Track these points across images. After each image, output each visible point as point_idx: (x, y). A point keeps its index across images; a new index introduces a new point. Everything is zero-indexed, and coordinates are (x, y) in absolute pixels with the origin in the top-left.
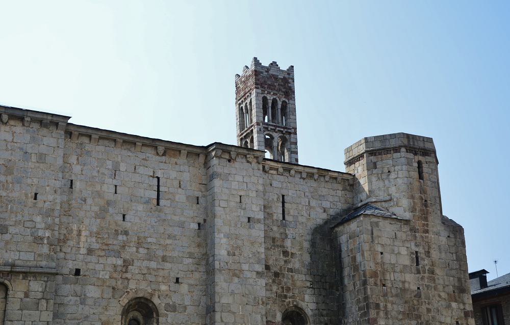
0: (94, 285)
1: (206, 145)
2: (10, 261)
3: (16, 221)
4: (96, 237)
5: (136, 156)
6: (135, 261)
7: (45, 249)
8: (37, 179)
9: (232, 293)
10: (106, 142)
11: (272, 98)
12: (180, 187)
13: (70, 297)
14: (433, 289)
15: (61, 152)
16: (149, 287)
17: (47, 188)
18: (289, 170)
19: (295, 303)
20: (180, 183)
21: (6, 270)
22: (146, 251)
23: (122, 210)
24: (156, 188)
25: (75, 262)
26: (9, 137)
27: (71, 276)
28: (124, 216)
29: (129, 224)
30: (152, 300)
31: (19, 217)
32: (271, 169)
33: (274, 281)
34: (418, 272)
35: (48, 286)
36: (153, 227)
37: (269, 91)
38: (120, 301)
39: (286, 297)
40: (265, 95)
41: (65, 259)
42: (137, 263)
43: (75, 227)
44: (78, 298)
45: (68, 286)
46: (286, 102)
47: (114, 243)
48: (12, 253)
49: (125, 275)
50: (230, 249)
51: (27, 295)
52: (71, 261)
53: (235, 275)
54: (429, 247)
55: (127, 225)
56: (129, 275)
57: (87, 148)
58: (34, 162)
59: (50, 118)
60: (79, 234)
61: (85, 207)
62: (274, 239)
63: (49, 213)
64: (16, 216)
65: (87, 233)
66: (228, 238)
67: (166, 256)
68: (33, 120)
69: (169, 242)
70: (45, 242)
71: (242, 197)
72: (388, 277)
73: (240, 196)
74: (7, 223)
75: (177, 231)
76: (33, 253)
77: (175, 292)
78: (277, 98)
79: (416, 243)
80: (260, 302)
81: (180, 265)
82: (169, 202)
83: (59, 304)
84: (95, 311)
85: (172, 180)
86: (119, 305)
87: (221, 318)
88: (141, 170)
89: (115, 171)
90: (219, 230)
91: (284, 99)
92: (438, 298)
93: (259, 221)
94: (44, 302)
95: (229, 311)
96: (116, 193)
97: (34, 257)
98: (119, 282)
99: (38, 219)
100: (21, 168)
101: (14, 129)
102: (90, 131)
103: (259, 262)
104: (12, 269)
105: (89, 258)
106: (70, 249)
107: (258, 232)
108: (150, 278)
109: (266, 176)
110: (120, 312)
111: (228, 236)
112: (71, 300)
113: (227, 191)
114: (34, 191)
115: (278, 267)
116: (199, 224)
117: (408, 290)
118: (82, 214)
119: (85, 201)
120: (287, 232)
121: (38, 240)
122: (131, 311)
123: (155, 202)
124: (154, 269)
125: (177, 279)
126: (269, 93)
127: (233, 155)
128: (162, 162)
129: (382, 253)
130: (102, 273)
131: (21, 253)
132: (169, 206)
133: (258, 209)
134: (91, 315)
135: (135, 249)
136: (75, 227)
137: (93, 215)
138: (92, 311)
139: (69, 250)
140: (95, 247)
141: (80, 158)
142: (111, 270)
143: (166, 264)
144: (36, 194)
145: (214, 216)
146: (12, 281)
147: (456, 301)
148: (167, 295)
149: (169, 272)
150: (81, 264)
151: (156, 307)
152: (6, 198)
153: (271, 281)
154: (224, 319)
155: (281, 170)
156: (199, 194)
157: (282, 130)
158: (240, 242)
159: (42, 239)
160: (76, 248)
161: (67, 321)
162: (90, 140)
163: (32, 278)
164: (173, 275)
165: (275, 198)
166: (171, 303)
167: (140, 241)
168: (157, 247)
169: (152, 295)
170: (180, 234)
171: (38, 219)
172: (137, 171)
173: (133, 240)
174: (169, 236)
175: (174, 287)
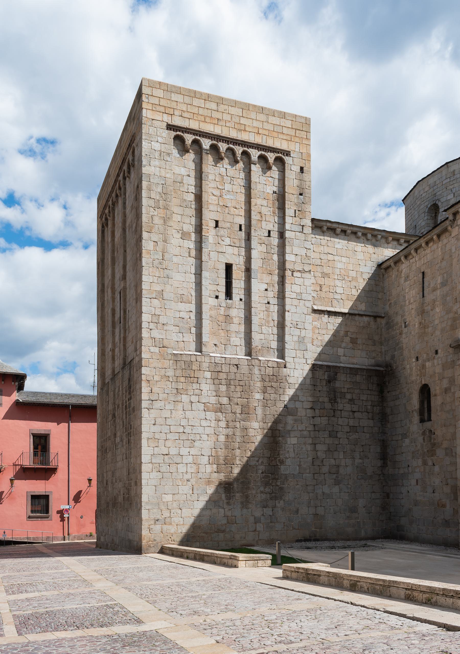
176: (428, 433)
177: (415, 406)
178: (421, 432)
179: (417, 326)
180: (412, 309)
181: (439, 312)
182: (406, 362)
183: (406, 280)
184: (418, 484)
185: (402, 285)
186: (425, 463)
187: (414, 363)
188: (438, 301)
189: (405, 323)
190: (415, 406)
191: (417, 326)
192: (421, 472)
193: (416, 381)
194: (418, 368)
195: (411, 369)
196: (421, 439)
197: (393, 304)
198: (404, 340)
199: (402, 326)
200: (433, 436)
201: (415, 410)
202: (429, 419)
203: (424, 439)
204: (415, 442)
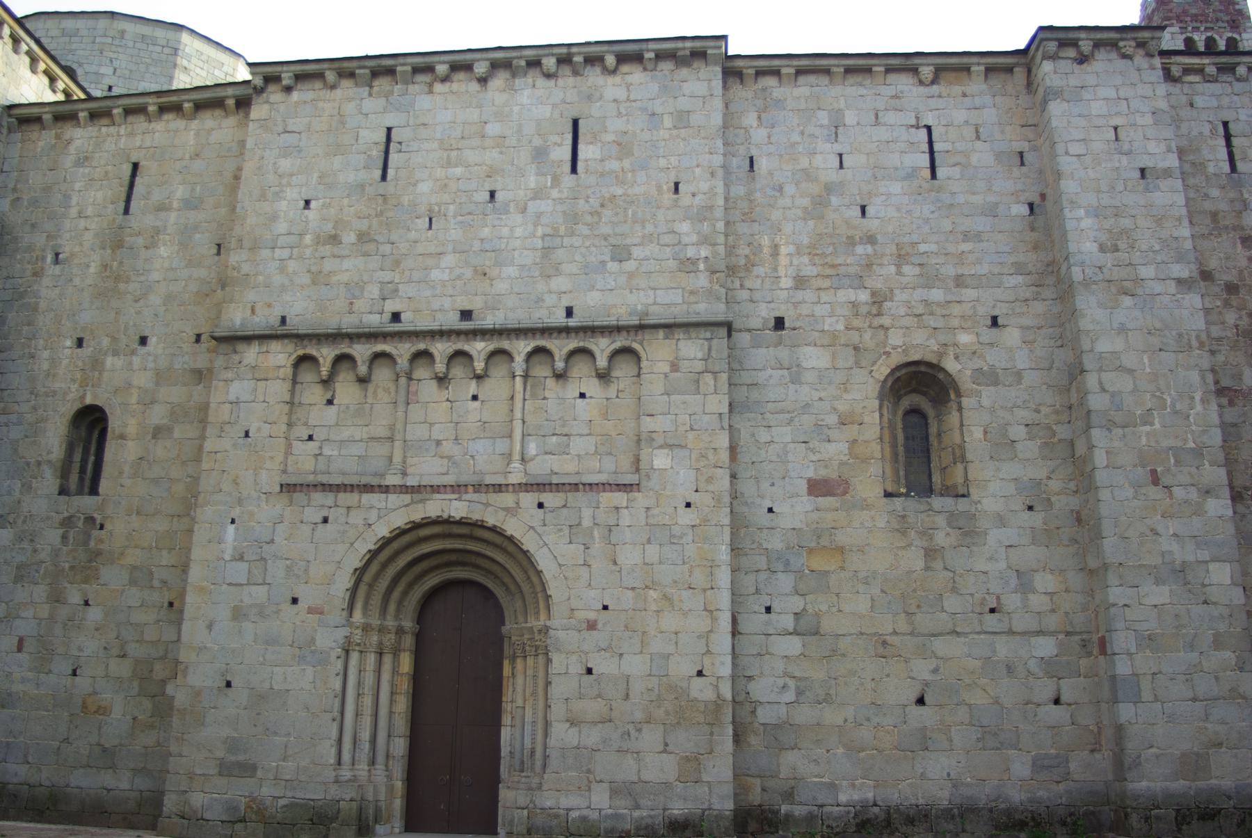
0: (815, 345)
1: (1022, 46)
2: (639, 307)
3: (643, 237)
4: (810, 254)
5: (876, 94)
6: (897, 292)
7: (702, 281)
8: (676, 157)
9: (1122, 330)
10: (812, 79)
11: (1204, 37)
12: (978, 138)
13: (769, 371)
15: (718, 103)
16: (933, 341)
17: (698, 170)
18: (1231, 69)
20: (977, 132)
21: (631, 323)
22: (917, 270)
23: (858, 198)
24: (925, 147)
25: (772, 305)
26: (621, 94)
27: (768, 332)
28: (863, 210)
29: (876, 223)
30: (942, 365)
31: (649, 228)
32: (1187, 71)
33: (1227, 304)
35: (714, 348)
36: (927, 221)
37: (1195, 25)
38: (872, 371)
41: (751, 301)
42: (900, 296)
43: (766, 241)
44: (785, 372)
45: (763, 351)
46: (1235, 39)
47: (848, 261)
48: (642, 293)
49: (877, 321)
50: (1104, 237)
51: (675, 367)
52: (766, 304)
55: (871, 224)
56: (886, 321)
57: (775, 94)
58: (670, 129)
59: (688, 44)
61: (781, 202)
62: (1214, 215)
63: (702, 215)
64: (644, 227)
65: (791, 249)
66: (1097, 216)
67: (963, 275)
68: (660, 56)
69: (966, 247)
70: (702, 266)
71: (1119, 129)
73: (1116, 129)
74: (628, 241)
75: (981, 224)
76: (680, 290)
77: (991, 344)
80: (1195, 343)
81: (999, 290)
82: (957, 169)
83: (748, 385)
84: (823, 394)
85: (959, 126)
86: (871, 380)
87: (1100, 383)
88: (890, 118)
89: (836, 127)
90: (1072, 202)
91: (1230, 35)
93: (1167, 173)
94: (708, 378)
95: (1120, 368)
96: (841, 166)
97: (683, 296)
98: (867, 336)
99: (685, 227)
100: (646, 142)
101: (629, 78)
102: (776, 62)
103: (1180, 258)
104: (643, 322)
105: (800, 295)
106: (759, 281)
107: (1170, 196)
108: (932, 322)
109: (1175, 89)
110: (876, 394)
111: (1097, 212)
112: (771, 377)
113: (1082, 122)
114: (673, 179)
116: (1031, 206)
118: (776, 215)
119: (781, 189)
120: (1246, 196)
121: (688, 266)
122: (906, 394)
123: (927, 173)
124: (938, 304)
126: (1196, 29)
127: (1086, 46)
128: (933, 97)
130: (828, 321)
131: (657, 291)
132: (958, 176)
133: (1163, 147)
134: (815, 403)
135: (893, 269)
136: (766, 241)
137: (799, 213)
138: (816, 395)
139: (757, 284)
140: (809, 273)
141: (763, 115)
142: (847, 313)
143: (964, 291)
144: (677, 185)
145: (1058, 175)
146: (645, 343)
148: (974, 353)
149: (974, 307)
150: (783, 307)
151: (953, 380)
152: (623, 198)
153: (1218, 303)
154: (1107, 387)
155: (1211, 70)
156: (1024, 146)
158: (1126, 223)
159: (693, 262)
160: (772, 280)
161: (768, 415)
162: (780, 79)
163: (681, 336)
164: (985, 311)
165: (1206, 129)
166: (985, 368)
167: (903, 252)
168: (941, 260)
169: (941, 355)
170: (988, 229)
171: (685, 227)
172: (880, 120)
173: (888, 251)
174: (965, 235)
175: (989, 334)
176: (80, 524)
177: (49, 452)
178: (58, 518)
179: (92, 270)
180: (87, 229)
181: (168, 257)
182: (41, 342)
183: (79, 163)
184: (24, 649)
185: (66, 170)
186: (57, 598)
187: (67, 350)
188: (169, 235)
189: (57, 255)
190: (49, 452)
191: (92, 270)
192: (41, 619)
193: (65, 394)
194: (80, 363)
195: (54, 361)
196: (53, 536)
197: (26, 203)
198: (46, 290)
199: (44, 258)
200: (96, 533)
201: (49, 462)
202: (94, 491)
203: (64, 537)
204: (32, 541)
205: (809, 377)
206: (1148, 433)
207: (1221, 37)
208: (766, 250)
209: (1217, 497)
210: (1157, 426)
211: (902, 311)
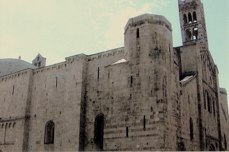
11: (188, 13)
14: (139, 93)
19: (101, 113)
32: (94, 58)
33: (93, 105)
34: (131, 86)
39: (97, 111)
40: (184, 13)
43: (35, 102)
51: (19, 125)
53: (70, 107)
54: (139, 71)
56: (47, 114)
60: (36, 104)
69: (59, 99)
72: (115, 93)
78: (190, 12)
79: (131, 71)
92: (141, 97)
115: (95, 99)
117: (124, 97)
124: (54, 110)
125: (60, 112)
126: (185, 11)
129: (113, 83)
136: (35, 102)
147: (152, 96)
157: (193, 24)
169: (53, 119)
205: (38, 125)
206: (69, 133)
207: (192, 12)
208: (35, 103)
209: (77, 144)
210: (71, 132)
211: (49, 112)
